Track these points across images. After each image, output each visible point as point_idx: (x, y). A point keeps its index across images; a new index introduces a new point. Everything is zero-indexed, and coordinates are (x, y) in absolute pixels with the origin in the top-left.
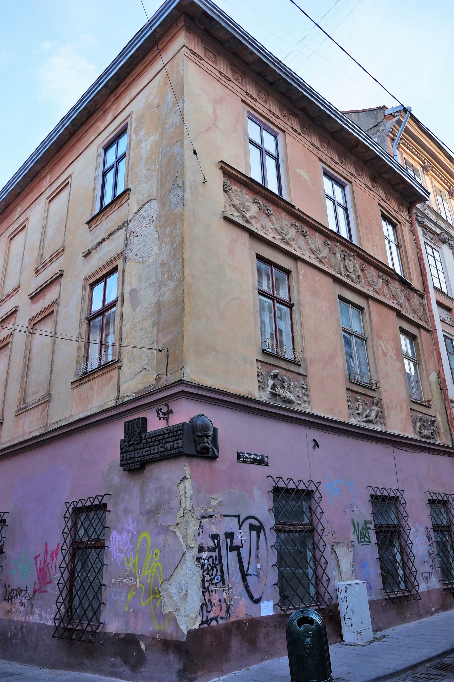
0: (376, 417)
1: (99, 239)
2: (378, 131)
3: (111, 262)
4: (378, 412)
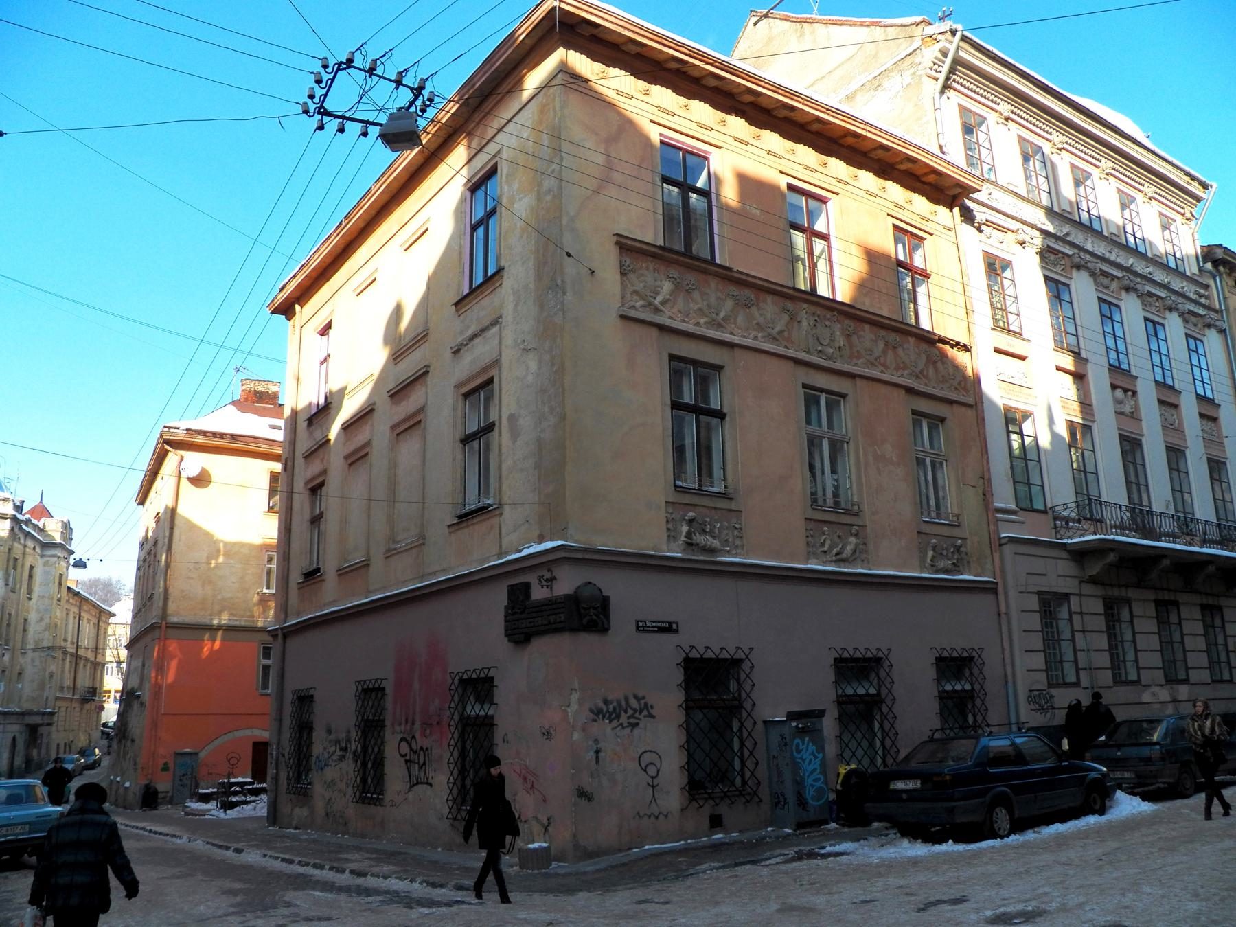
0: (855, 551)
1: (470, 332)
2: (911, 65)
3: (485, 369)
4: (857, 545)
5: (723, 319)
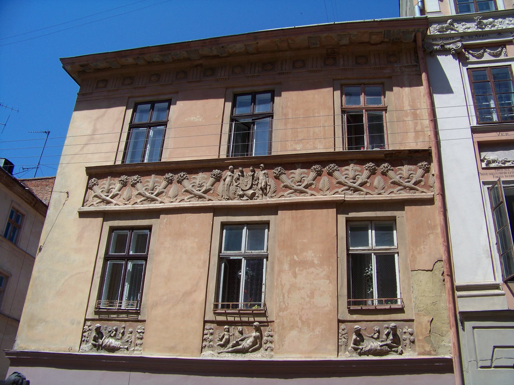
5: (157, 195)
